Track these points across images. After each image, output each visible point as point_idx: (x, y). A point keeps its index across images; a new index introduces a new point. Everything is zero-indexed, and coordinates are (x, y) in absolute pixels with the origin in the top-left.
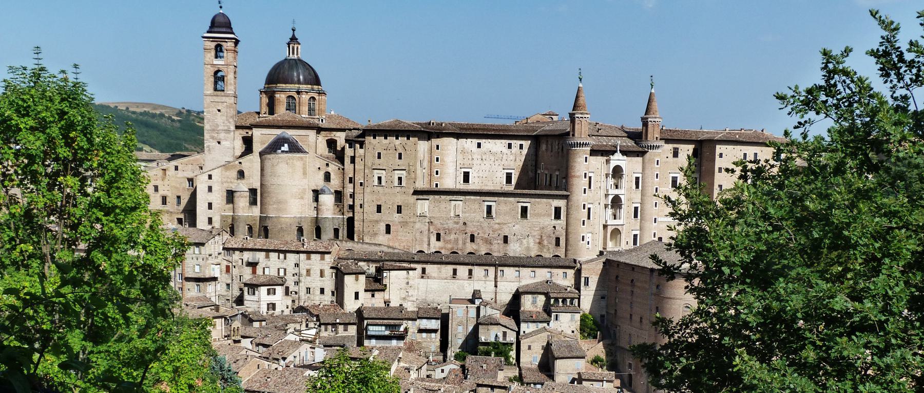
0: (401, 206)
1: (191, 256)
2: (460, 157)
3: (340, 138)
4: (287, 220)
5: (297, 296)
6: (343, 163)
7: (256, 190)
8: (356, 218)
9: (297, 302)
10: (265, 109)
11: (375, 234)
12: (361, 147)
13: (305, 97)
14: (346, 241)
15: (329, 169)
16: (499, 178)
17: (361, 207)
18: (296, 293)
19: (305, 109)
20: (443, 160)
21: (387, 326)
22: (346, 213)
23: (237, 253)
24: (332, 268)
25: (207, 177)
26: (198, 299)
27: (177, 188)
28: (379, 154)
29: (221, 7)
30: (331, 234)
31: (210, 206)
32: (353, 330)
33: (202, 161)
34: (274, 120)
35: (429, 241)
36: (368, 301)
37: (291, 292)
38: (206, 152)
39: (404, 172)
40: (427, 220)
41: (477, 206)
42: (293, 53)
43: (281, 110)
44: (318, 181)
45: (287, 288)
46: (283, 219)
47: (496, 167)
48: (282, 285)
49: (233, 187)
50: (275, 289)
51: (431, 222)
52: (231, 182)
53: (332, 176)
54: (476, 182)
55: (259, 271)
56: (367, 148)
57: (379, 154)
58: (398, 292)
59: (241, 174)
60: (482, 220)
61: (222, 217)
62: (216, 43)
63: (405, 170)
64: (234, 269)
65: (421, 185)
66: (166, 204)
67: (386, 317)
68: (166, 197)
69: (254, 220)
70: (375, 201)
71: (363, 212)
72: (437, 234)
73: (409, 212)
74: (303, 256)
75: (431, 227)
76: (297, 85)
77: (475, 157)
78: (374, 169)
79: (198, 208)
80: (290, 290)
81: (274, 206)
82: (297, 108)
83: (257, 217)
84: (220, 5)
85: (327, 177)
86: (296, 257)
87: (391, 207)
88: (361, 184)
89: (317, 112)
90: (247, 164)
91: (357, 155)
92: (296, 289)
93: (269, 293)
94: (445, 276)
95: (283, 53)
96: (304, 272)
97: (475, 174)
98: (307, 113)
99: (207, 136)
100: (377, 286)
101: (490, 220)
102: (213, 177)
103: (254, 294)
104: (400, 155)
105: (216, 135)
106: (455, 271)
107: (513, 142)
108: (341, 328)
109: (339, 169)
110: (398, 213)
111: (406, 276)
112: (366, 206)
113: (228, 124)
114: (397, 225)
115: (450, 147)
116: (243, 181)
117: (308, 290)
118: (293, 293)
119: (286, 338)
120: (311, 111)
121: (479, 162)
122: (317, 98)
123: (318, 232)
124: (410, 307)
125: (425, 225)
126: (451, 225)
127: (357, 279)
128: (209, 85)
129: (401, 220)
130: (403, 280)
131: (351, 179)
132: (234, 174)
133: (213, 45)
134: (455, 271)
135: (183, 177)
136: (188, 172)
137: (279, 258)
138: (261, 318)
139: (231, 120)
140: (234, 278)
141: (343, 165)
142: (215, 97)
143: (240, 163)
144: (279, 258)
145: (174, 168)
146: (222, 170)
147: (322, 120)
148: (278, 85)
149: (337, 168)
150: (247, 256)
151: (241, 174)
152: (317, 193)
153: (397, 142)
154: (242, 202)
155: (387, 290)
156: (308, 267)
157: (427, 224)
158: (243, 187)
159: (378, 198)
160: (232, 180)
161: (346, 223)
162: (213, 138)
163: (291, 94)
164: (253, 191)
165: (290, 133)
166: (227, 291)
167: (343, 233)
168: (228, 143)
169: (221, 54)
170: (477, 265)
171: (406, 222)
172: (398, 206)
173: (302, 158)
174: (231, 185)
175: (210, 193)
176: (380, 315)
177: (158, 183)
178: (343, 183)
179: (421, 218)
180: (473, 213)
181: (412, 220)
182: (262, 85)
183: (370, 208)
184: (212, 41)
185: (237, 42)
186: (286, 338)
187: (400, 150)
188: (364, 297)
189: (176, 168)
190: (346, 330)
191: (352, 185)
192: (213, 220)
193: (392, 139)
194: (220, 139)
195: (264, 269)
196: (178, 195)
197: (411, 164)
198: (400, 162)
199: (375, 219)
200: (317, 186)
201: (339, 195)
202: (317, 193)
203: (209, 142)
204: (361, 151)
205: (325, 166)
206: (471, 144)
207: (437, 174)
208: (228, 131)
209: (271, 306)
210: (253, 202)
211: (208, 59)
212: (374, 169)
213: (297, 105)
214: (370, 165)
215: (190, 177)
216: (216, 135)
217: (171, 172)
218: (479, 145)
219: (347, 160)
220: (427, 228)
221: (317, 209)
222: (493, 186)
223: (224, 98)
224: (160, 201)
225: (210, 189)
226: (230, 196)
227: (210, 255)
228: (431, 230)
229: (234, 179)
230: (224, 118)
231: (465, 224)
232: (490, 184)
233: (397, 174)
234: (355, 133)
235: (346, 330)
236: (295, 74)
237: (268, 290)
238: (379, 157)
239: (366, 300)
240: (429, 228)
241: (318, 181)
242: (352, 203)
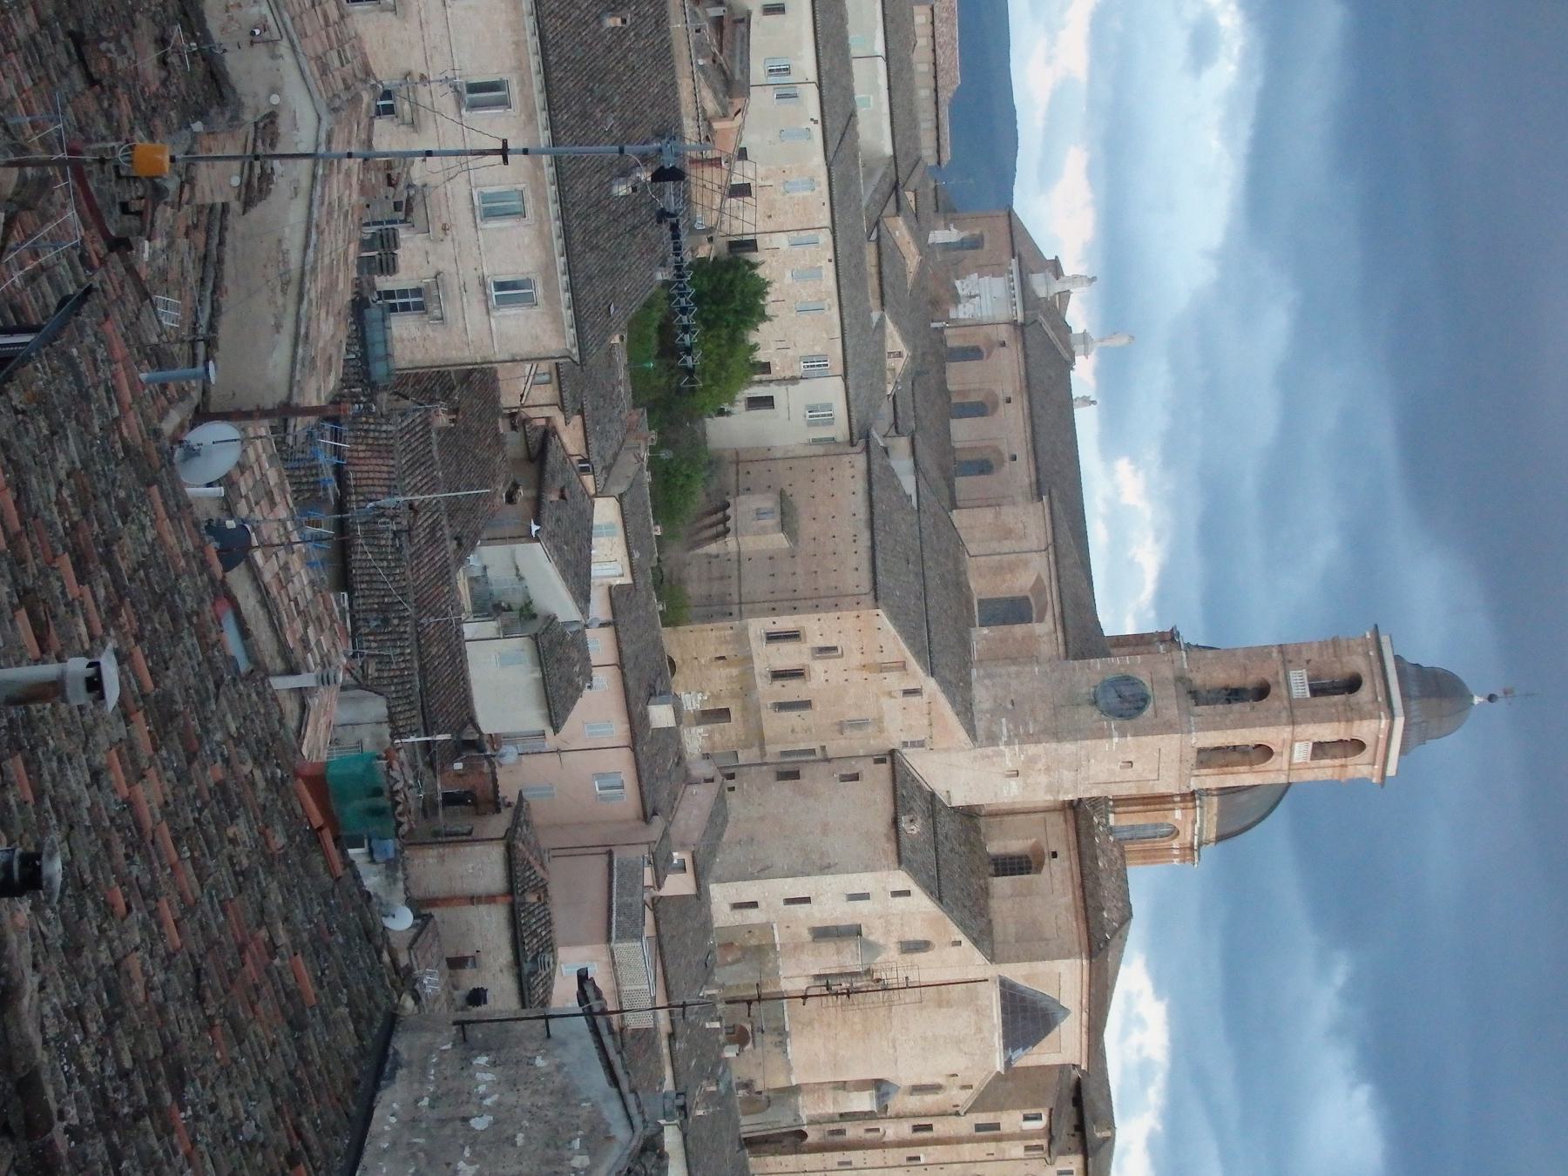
8: (806, 1157)
17: (840, 1164)
52: (887, 933)
71: (825, 1170)
84: (1499, 694)
91: (1003, 1145)
143: (959, 943)
149: (960, 1103)
175: (845, 898)
216: (1040, 766)
217: (895, 681)
230: (1103, 777)
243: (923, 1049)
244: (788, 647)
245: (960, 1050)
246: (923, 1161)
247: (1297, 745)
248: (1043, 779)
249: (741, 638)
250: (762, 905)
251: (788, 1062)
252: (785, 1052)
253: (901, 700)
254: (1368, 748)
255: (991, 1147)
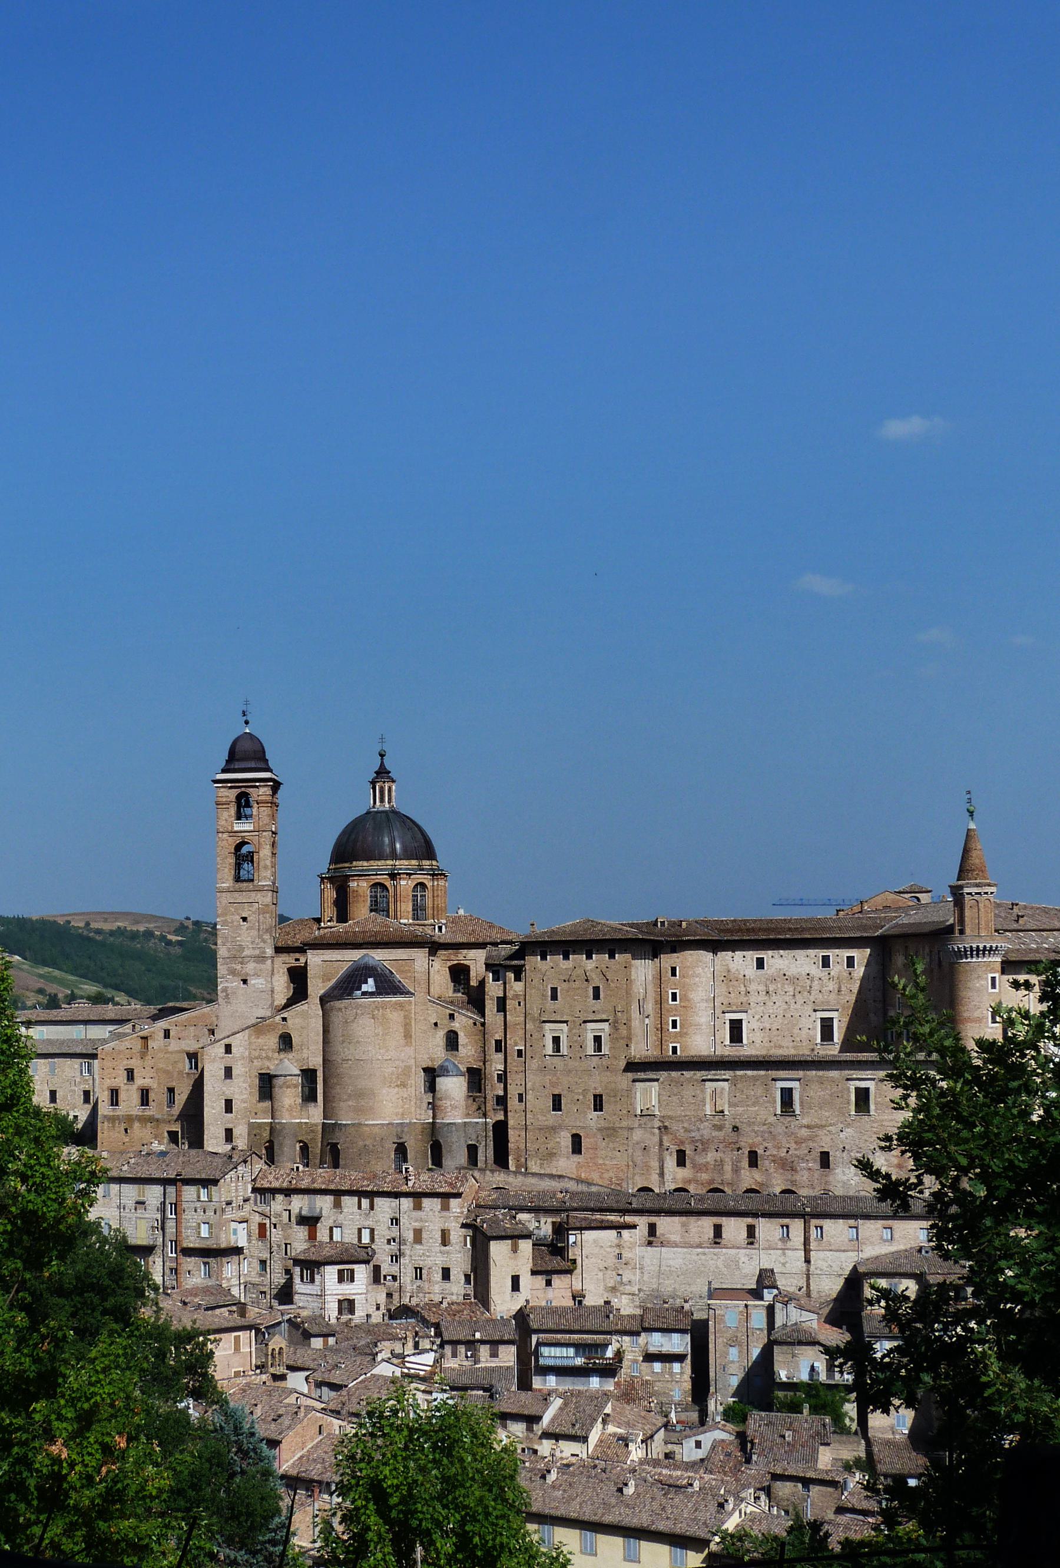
0: (601, 1096)
1: (193, 1205)
2: (722, 989)
3: (476, 961)
4: (376, 1130)
5: (397, 1284)
6: (481, 1011)
7: (315, 1071)
9: (396, 1296)
10: (330, 911)
11: (551, 1155)
12: (518, 979)
13: (406, 884)
14: (492, 1171)
15: (456, 1025)
16: (805, 1031)
17: (521, 1100)
18: (394, 1278)
19: (407, 907)
20: (685, 998)
21: (578, 1347)
22: (490, 1113)
23: (280, 1197)
24: (464, 1226)
25: (223, 1050)
26: (206, 1291)
27: (167, 1072)
28: (554, 991)
29: (247, 722)
30: (462, 1158)
31: (229, 1106)
32: (508, 1356)
33: (214, 1019)
34: (346, 932)
35: (662, 1168)
36: (540, 1294)
37: (385, 1277)
38: (220, 1000)
39: (605, 1026)
40: (657, 1124)
41: (760, 1091)
42: (382, 800)
43: (361, 912)
44: (435, 1050)
45: (377, 1269)
46: (367, 1129)
47: (798, 1006)
48: (367, 1262)
49: (272, 1067)
50: (352, 1271)
51: (666, 1128)
52: (268, 1058)
53: (462, 1039)
54: (758, 1041)
55: (322, 1235)
56: (529, 980)
57: (554, 991)
58: (601, 1274)
59: (286, 1042)
60: (772, 1119)
61: (251, 1126)
62: (239, 791)
63: (607, 1021)
64: (273, 1230)
65: (642, 1049)
66: (147, 1105)
67: (577, 1327)
68: (147, 1091)
69: (312, 1131)
70: (548, 1085)
71: (525, 1111)
72: (678, 1151)
73: (619, 1107)
74: (406, 1203)
75: (665, 1138)
76: (390, 862)
77: (753, 987)
78: (544, 1022)
79: (206, 1109)
80: (383, 1273)
81: (350, 1103)
82: (392, 906)
83: (316, 1125)
84: (245, 718)
85: (452, 1041)
86: (393, 1204)
87: (581, 1097)
88: (520, 1052)
89: (429, 911)
90: (297, 1021)
91: (509, 994)
92: (394, 1270)
93: (341, 1280)
94: (697, 1240)
95: (364, 801)
96: (409, 1236)
97: (755, 1025)
98: (410, 916)
99: (222, 969)
100: (556, 1262)
101: (789, 1119)
102: (234, 1050)
103: (312, 1281)
104: (596, 990)
105: (238, 967)
106: (718, 1230)
107: (831, 953)
108: (484, 1351)
109: (475, 1024)
110: (595, 1110)
111: (616, 1241)
112: (530, 1097)
113: (262, 945)
114: (594, 1136)
115: (699, 970)
116: (290, 1056)
117: (419, 1272)
118: (389, 1278)
119: (375, 1371)
120: (418, 911)
121: (763, 997)
122: (429, 884)
123: (437, 1155)
124: (626, 1307)
125: (654, 1134)
126: (706, 1131)
127: (515, 1249)
128: (226, 870)
129: (603, 1124)
130: (608, 1250)
131: (498, 1043)
132: (272, 1041)
133: (232, 794)
134: (718, 1230)
135: (179, 1052)
136: (187, 1041)
137: (360, 1207)
138: (325, 1331)
139: (267, 937)
140: (275, 1248)
141: (483, 1016)
142: (236, 894)
143: (284, 1019)
144: (360, 1207)
145: (162, 1034)
146: (250, 1036)
147: (440, 928)
148: (354, 863)
150: (299, 1204)
151: (286, 1042)
152: (432, 1075)
153: (590, 965)
154: (289, 1096)
155: (578, 1270)
156: (417, 1225)
157: (657, 1131)
158: (290, 1066)
159: (554, 1079)
160: (270, 1054)
161: (491, 1134)
162: (233, 972)
163: (380, 879)
164: (309, 1075)
165: (379, 956)
166: (261, 1275)
167: (486, 1153)
168: (261, 981)
169: (248, 811)
170: (764, 1215)
171: (614, 1129)
172: (595, 1096)
173: (401, 1005)
174: (267, 1063)
175: (228, 1081)
176: (564, 1324)
177: (134, 1063)
178: (484, 1051)
179: (644, 1119)
180: (754, 1104)
181: (624, 1124)
182: (323, 864)
183: (539, 1103)
184: (231, 788)
185: (276, 786)
186: (375, 1371)
187: (597, 981)
188: (530, 1287)
189: (167, 1034)
190: (494, 1355)
191: (501, 1056)
192: (236, 1132)
193: (578, 959)
194: (247, 975)
195: (331, 1229)
196: (170, 1085)
197: (619, 1008)
198: (597, 1005)
199: (550, 1123)
200: (432, 1060)
201: (476, 1078)
202: (432, 1075)
203: (226, 982)
204: (517, 987)
205: (446, 1021)
206: (741, 962)
207: (674, 1026)
208: (261, 958)
209: (345, 1305)
210: (310, 1097)
211: (224, 822)
212: (544, 1022)
213: (392, 900)
214: (536, 1012)
215: (191, 1050)
216: (238, 967)
217: (157, 1043)
218: (760, 964)
219: (491, 1006)
220: (656, 1139)
221: (433, 1106)
222: (794, 1047)
223: (253, 894)
224: (136, 1098)
225: (228, 1072)
226: (267, 1085)
227: (229, 1203)
228: (666, 1144)
229: (273, 1051)
230: (254, 933)
231: (735, 1129)
232: (787, 1042)
233: (591, 1030)
234: (505, 950)
235: (494, 1355)
236: (386, 840)
237: (340, 1272)
238: (554, 997)
239: (532, 1290)
240: (661, 1141)
241: (435, 1050)
242: (501, 1093)
243: (350, 1043)
244: (122, 1096)
245: (353, 1021)
246: (523, 1048)
247: (236, 829)
248: (251, 967)
249: (112, 1119)
250: (229, 1126)
251: (353, 1125)
252: (345, 1125)
253: (171, 1040)
254: (243, 789)
255: (510, 1004)
